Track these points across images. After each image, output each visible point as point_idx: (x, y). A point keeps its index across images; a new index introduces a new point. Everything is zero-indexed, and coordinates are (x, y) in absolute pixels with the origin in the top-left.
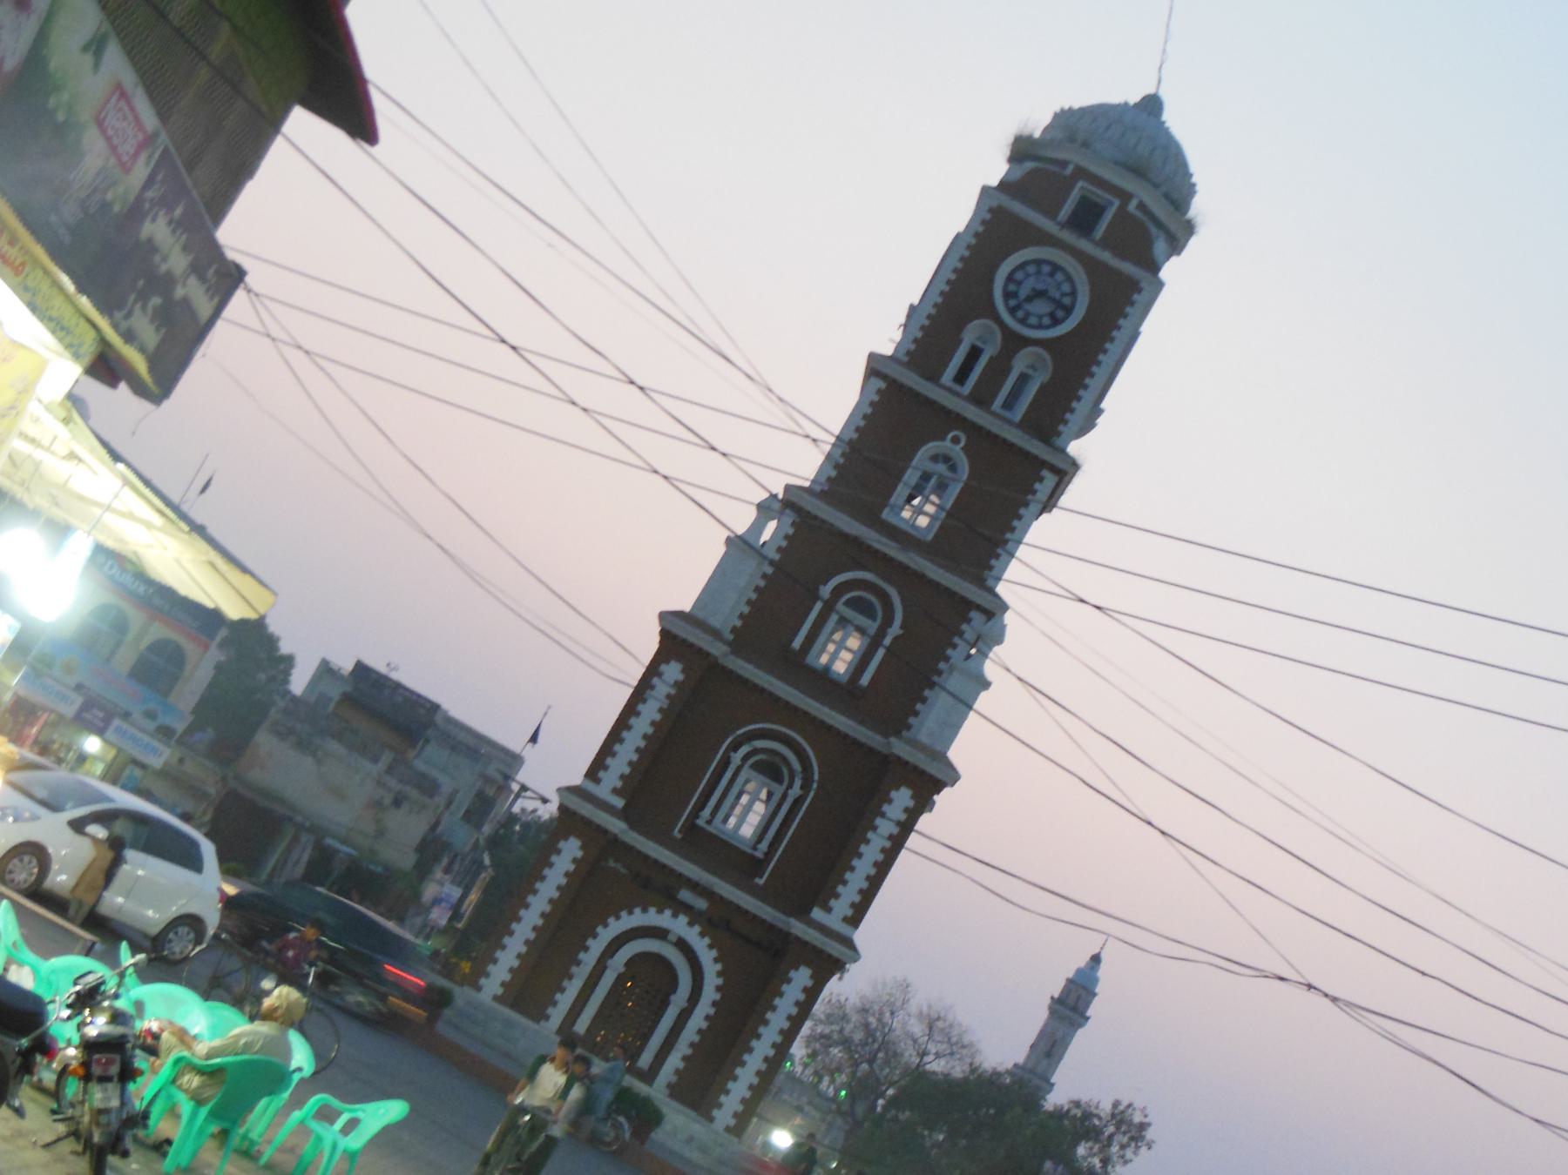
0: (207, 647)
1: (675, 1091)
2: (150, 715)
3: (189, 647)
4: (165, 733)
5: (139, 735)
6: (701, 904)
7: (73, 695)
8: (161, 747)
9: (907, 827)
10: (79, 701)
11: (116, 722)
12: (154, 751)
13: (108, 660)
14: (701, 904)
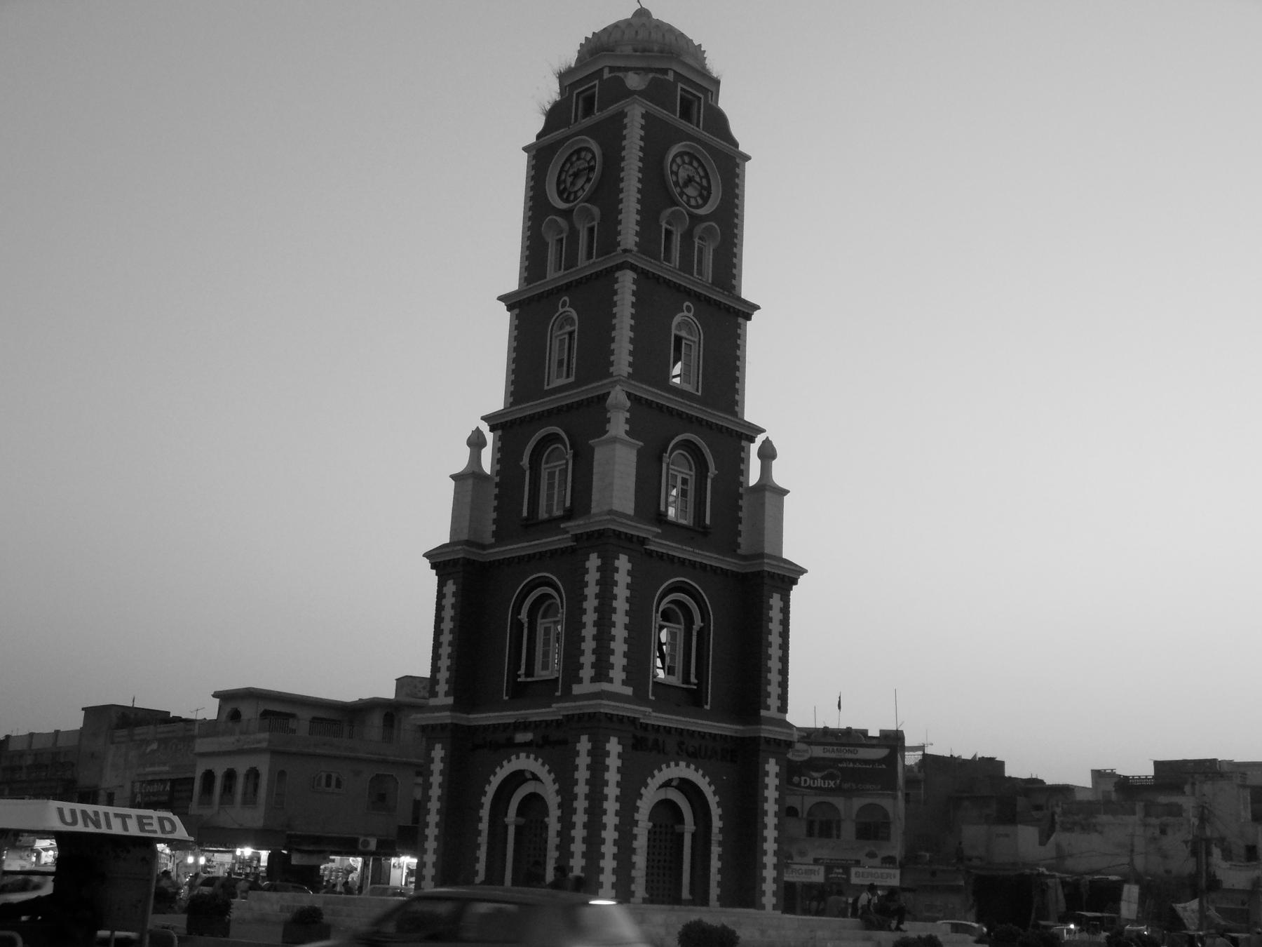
0: (895, 798)
1: (725, 901)
2: (872, 855)
3: (886, 803)
4: (889, 861)
5: (874, 871)
6: (529, 736)
7: (816, 868)
8: (892, 871)
9: (785, 610)
10: (822, 869)
11: (853, 870)
12: (889, 876)
13: (838, 837)
14: (529, 736)
